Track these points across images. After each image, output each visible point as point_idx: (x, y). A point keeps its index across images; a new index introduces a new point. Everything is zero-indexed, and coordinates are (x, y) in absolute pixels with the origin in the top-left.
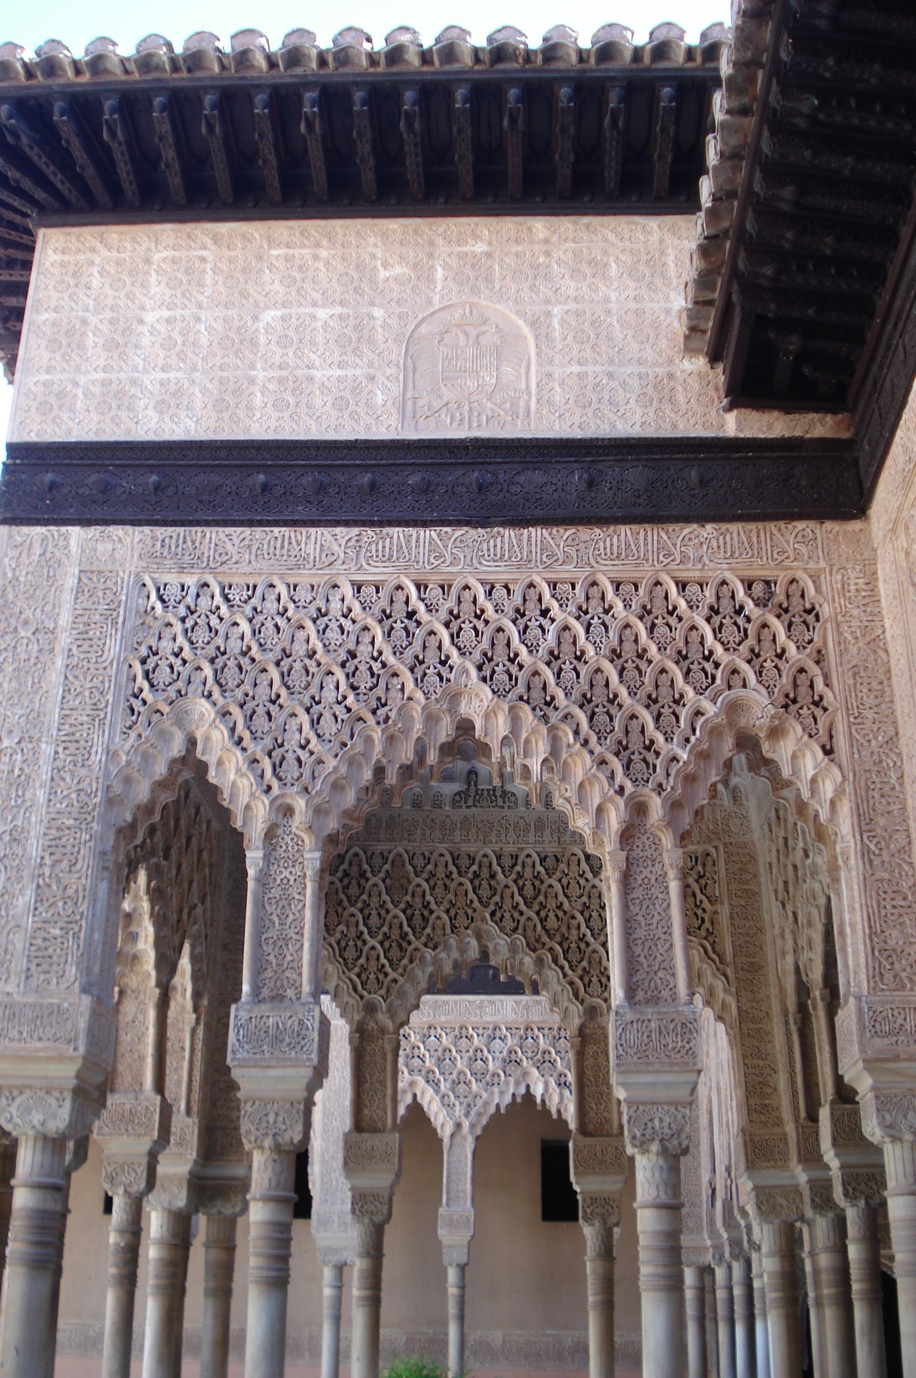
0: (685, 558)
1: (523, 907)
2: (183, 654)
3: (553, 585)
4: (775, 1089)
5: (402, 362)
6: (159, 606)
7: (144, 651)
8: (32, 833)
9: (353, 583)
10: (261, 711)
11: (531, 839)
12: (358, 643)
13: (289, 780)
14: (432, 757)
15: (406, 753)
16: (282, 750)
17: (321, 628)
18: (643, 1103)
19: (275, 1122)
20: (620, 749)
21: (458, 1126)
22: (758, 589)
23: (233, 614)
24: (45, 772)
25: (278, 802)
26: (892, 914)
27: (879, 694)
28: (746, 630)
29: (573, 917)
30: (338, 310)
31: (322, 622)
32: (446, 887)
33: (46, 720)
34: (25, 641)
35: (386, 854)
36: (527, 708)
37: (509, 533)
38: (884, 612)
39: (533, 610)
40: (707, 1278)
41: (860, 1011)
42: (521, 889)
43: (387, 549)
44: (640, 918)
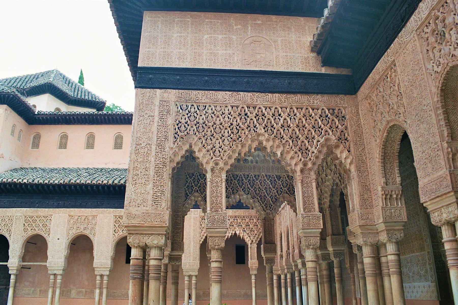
1: (250, 188)
2: (188, 123)
6: (181, 110)
8: (151, 169)
10: (209, 138)
11: (252, 171)
12: (233, 121)
14: (253, 150)
16: (215, 148)
18: (308, 236)
22: (331, 111)
24: (153, 153)
28: (328, 121)
29: (263, 191)
30: (224, 36)
31: (223, 115)
32: (231, 183)
34: (146, 119)
36: (277, 139)
39: (277, 114)
42: (250, 183)
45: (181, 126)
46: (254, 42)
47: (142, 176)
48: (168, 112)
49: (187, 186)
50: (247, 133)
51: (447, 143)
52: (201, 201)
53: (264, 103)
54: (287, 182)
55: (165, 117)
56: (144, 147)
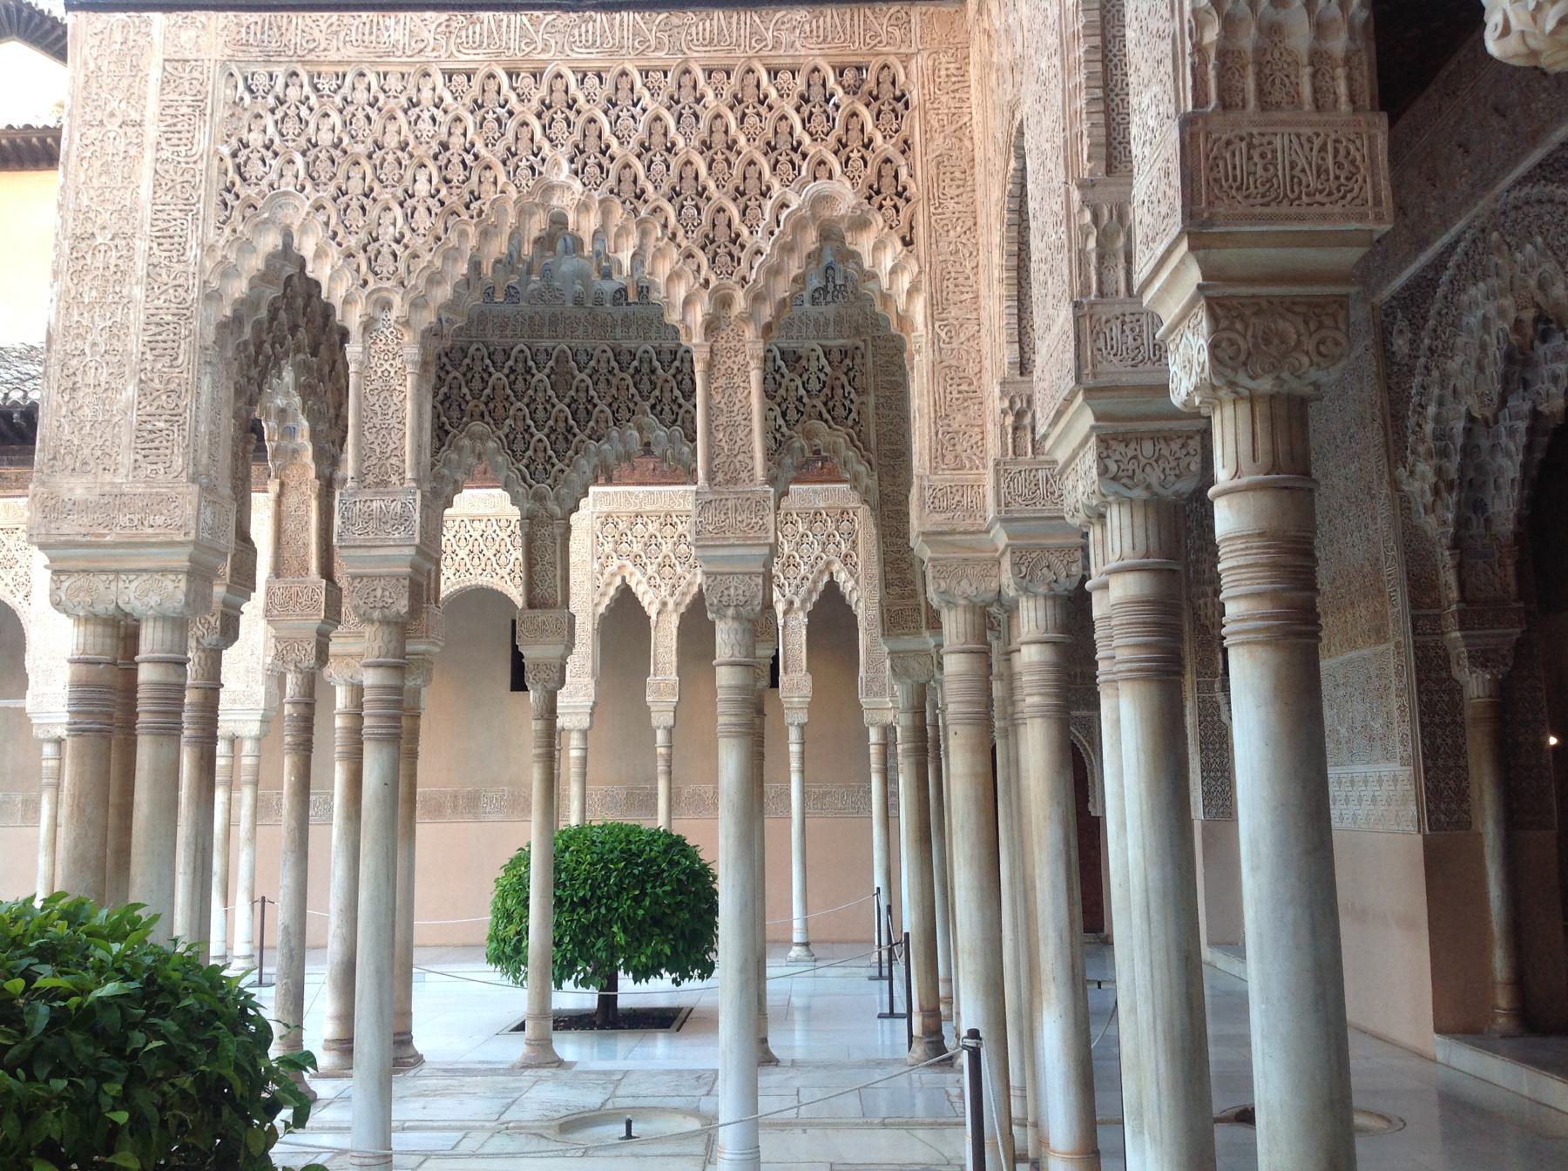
0: (777, 44)
2: (274, 147)
3: (645, 73)
4: (911, 565)
6: (247, 97)
8: (132, 330)
9: (444, 72)
10: (355, 204)
12: (450, 134)
13: (385, 274)
14: (527, 250)
15: (499, 246)
16: (377, 245)
17: (412, 119)
19: (383, 596)
21: (664, 604)
22: (849, 75)
25: (375, 296)
26: (957, 399)
27: (961, 183)
31: (414, 112)
33: (139, 216)
35: (550, 350)
36: (617, 201)
37: (601, 18)
38: (973, 99)
40: (891, 736)
41: (922, 488)
42: (679, 384)
44: (722, 405)
45: (249, 158)
47: (98, 358)
48: (198, 107)
49: (440, 397)
50: (502, 179)
51: (1080, 187)
53: (575, 56)
54: (822, 376)
55: (186, 127)
56: (103, 248)
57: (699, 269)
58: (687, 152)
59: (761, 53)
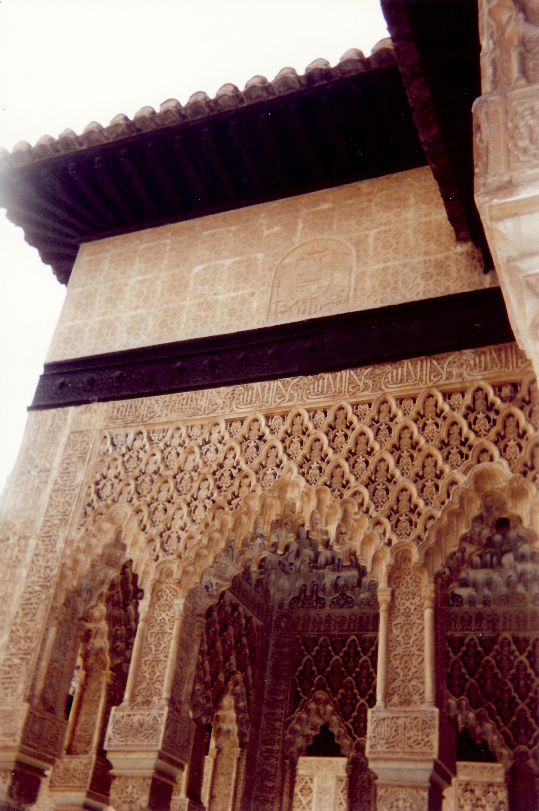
0: (450, 376)
3: (355, 406)
5: (271, 281)
6: (111, 448)
7: (98, 477)
9: (227, 421)
14: (265, 529)
15: (248, 528)
19: (132, 793)
20: (392, 514)
22: (506, 391)
23: (152, 448)
25: (162, 567)
30: (238, 258)
37: (328, 376)
43: (250, 397)
44: (400, 639)
46: (307, 257)
50: (254, 482)
52: (333, 713)
57: (384, 533)
58: (382, 453)
59: (438, 383)
